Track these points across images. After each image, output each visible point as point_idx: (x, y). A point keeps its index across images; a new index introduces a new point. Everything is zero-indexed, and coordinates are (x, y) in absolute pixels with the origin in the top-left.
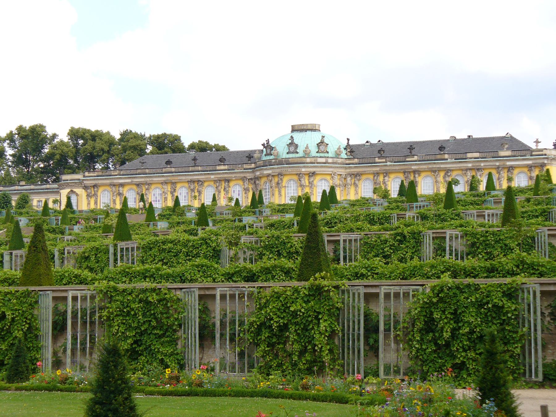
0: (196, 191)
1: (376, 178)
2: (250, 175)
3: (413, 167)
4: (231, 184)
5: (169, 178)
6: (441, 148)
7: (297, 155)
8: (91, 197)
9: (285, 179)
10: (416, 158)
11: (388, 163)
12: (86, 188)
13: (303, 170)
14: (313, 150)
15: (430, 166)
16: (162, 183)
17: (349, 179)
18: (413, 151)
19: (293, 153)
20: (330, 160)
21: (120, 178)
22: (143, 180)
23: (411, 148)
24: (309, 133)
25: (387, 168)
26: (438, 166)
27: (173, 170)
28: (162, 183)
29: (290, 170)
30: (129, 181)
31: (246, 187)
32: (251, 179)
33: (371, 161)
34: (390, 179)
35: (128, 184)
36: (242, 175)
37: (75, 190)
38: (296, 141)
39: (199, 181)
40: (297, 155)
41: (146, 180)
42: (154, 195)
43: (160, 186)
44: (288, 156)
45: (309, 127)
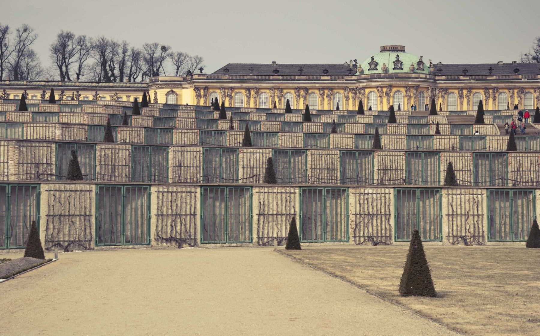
2: (352, 85)
3: (492, 85)
5: (277, 85)
7: (402, 71)
8: (200, 98)
10: (495, 77)
11: (471, 81)
12: (197, 89)
13: (410, 83)
20: (428, 77)
21: (231, 83)
23: (491, 69)
27: (280, 77)
29: (399, 83)
30: (239, 85)
32: (353, 89)
33: (456, 78)
37: (174, 90)
39: (306, 88)
40: (402, 71)
43: (268, 91)
44: (394, 71)
45: (399, 48)
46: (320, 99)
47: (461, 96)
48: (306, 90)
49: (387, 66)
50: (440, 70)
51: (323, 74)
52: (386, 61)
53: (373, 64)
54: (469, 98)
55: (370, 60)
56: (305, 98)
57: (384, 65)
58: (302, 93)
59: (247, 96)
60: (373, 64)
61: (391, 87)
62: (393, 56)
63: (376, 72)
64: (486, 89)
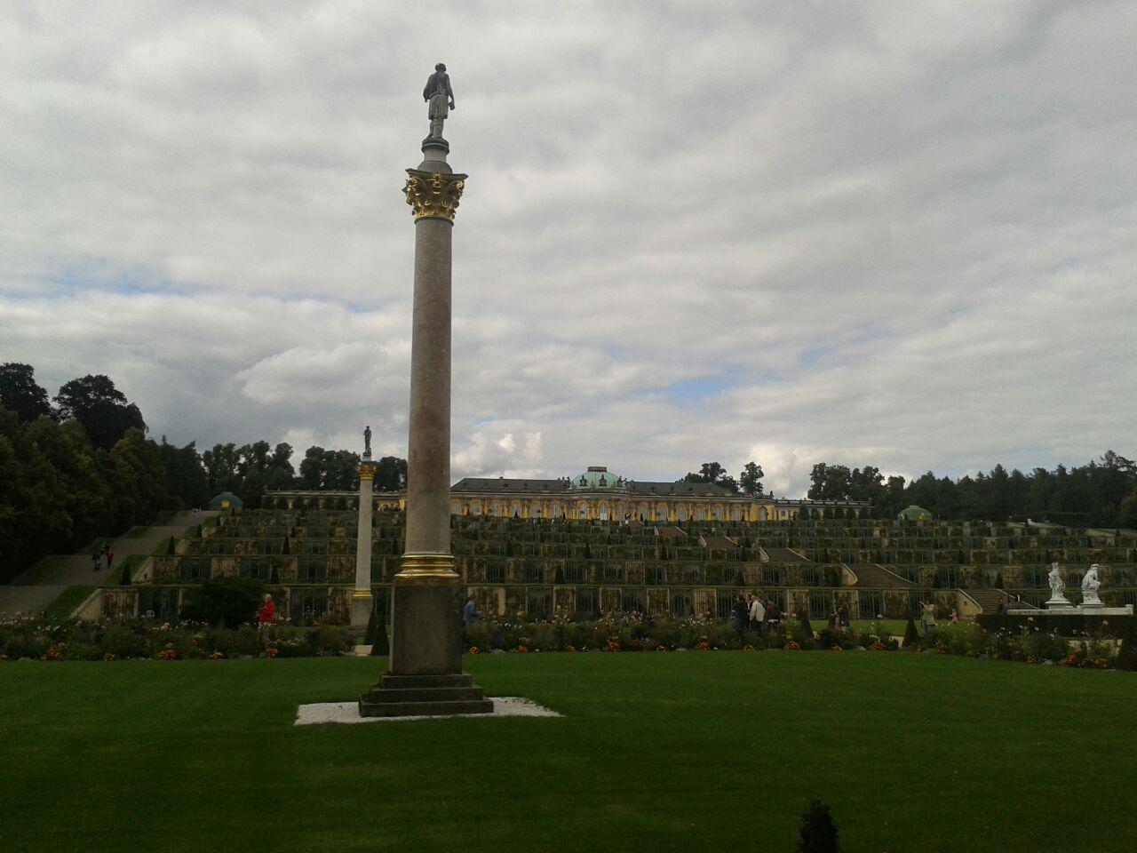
4: (552, 502)
47: (650, 508)
48: (530, 500)
52: (594, 478)
56: (529, 508)
60: (584, 481)
61: (597, 499)
62: (599, 475)
64: (669, 503)
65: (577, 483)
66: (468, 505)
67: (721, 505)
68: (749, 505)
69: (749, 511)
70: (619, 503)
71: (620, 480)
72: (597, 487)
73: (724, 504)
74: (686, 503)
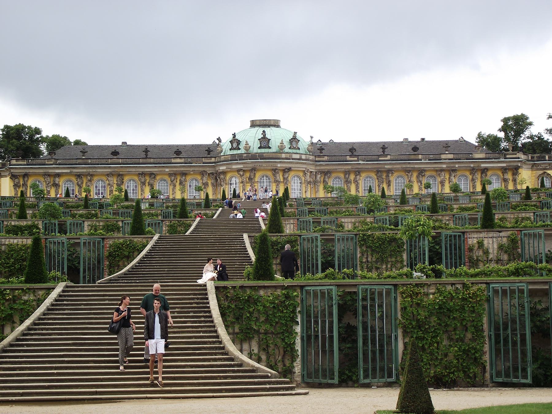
0: (147, 184)
1: (347, 176)
2: (210, 169)
4: (189, 178)
5: (116, 170)
6: (415, 149)
7: (270, 151)
9: (258, 175)
10: (389, 157)
13: (279, 165)
14: (287, 145)
15: (404, 166)
16: (108, 175)
17: (319, 176)
18: (386, 150)
19: (264, 148)
20: (304, 157)
22: (85, 170)
23: (384, 147)
24: (273, 128)
25: (360, 167)
26: (412, 166)
27: (120, 161)
28: (108, 175)
29: (264, 165)
31: (204, 182)
32: (212, 174)
34: (361, 178)
35: (66, 174)
36: (201, 169)
38: (267, 136)
40: (270, 151)
41: (88, 171)
42: (96, 187)
43: (104, 178)
44: (260, 151)
45: (272, 123)
46: (171, 187)
47: (347, 182)
48: (152, 175)
49: (251, 144)
50: (321, 149)
51: (175, 156)
52: (251, 138)
53: (235, 142)
54: (358, 183)
55: (231, 137)
57: (247, 144)
58: (148, 179)
59: (78, 185)
60: (235, 142)
63: (239, 152)
64: (378, 172)
65: (226, 145)
66: (56, 185)
67: (468, 173)
68: (515, 170)
69: (514, 180)
70: (292, 174)
71: (294, 140)
72: (255, 148)
73: (473, 171)
74: (408, 171)
